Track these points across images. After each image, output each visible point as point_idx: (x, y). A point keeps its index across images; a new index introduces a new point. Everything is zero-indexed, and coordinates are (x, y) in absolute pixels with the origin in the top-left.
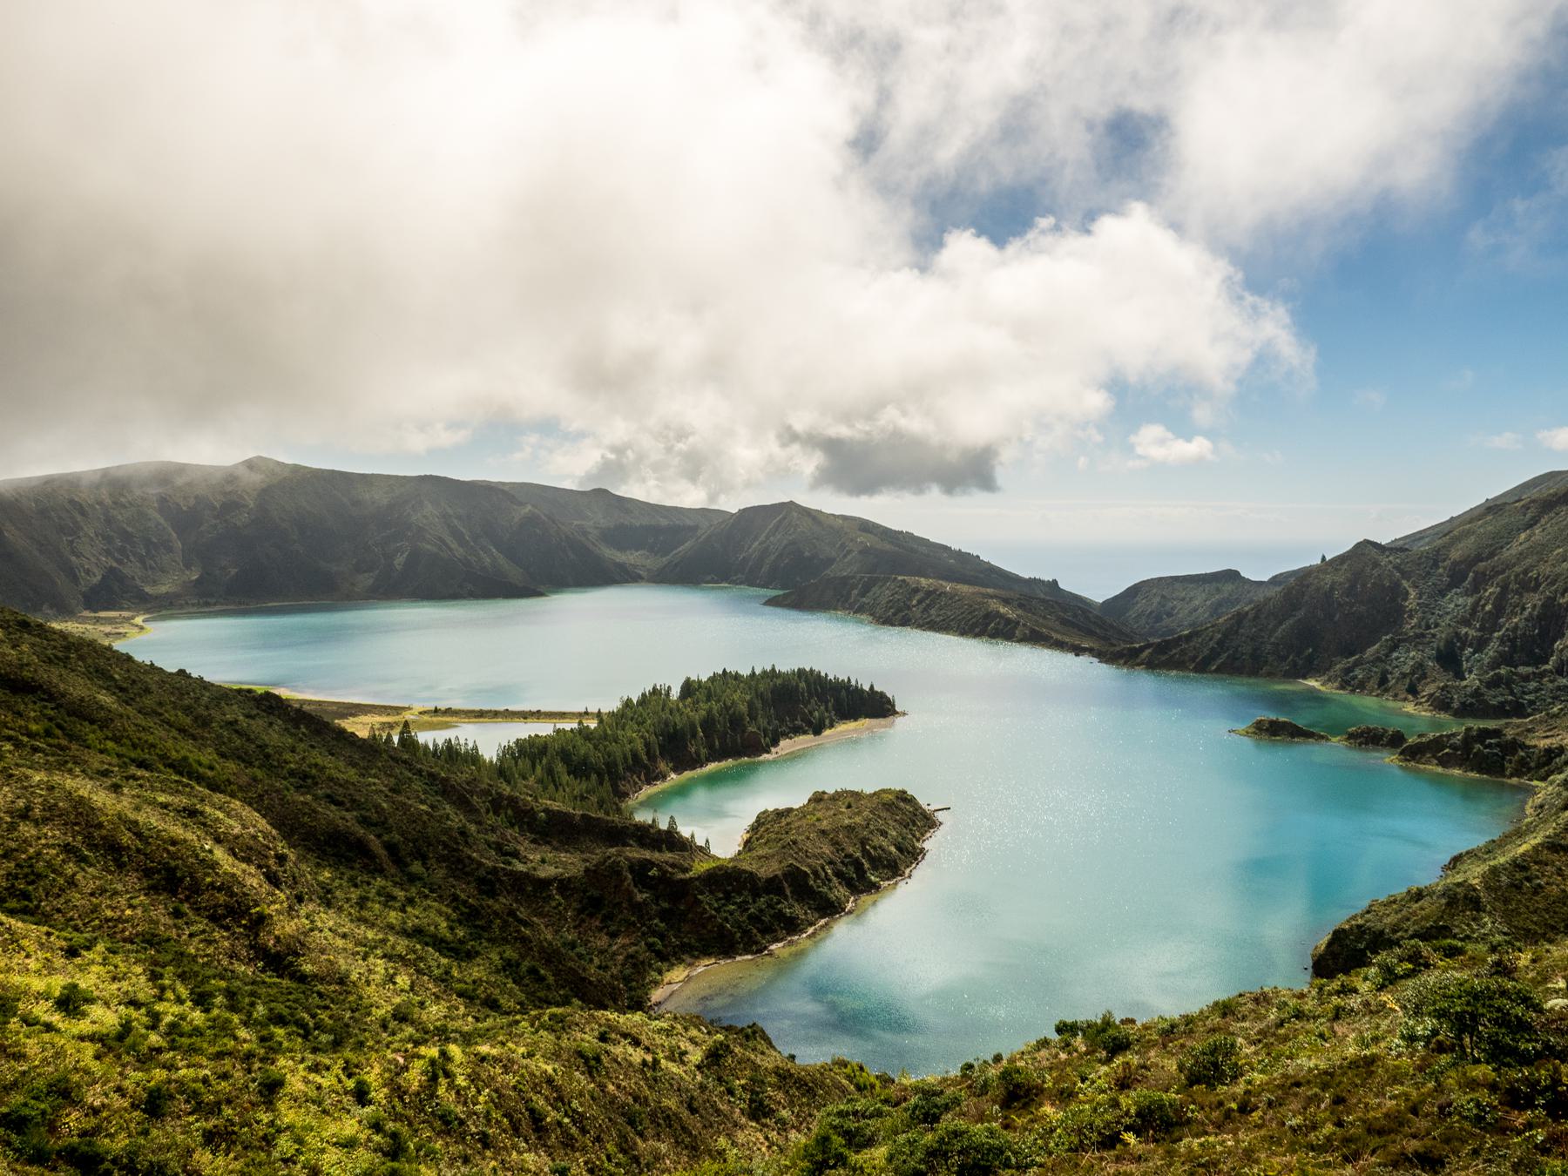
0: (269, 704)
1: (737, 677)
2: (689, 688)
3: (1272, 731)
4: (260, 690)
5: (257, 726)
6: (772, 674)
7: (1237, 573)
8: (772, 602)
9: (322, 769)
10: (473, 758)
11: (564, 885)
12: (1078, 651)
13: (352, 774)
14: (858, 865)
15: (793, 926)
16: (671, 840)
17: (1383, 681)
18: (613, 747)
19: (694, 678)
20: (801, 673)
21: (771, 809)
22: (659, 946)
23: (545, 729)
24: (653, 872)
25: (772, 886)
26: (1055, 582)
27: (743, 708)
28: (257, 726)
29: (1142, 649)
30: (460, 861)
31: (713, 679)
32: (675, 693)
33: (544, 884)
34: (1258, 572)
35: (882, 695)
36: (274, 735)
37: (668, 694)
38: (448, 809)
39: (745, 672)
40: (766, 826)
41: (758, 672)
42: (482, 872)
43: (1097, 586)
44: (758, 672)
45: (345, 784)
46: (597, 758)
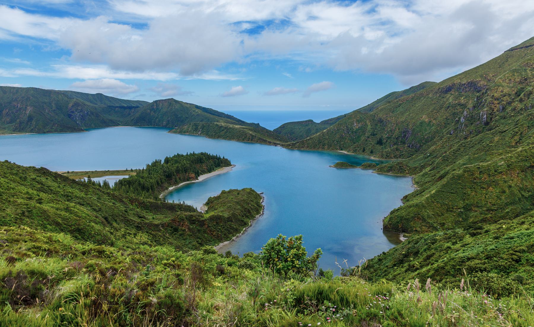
0: (43, 171)
1: (182, 156)
2: (167, 160)
4: (38, 167)
5: (43, 179)
6: (194, 154)
7: (312, 121)
9: (73, 193)
11: (163, 225)
12: (276, 145)
13: (83, 194)
14: (249, 212)
15: (237, 231)
16: (190, 209)
17: (364, 151)
18: (151, 181)
20: (202, 154)
21: (212, 197)
22: (200, 241)
24: (194, 218)
25: (229, 219)
26: (258, 124)
27: (188, 165)
28: (43, 179)
29: (295, 143)
30: (128, 221)
31: (175, 156)
32: (162, 162)
33: (157, 226)
35: (227, 160)
36: (50, 182)
38: (118, 204)
39: (185, 154)
40: (210, 203)
41: (189, 154)
42: (136, 224)
43: (272, 126)
44: (189, 154)
45: (82, 198)
46: (147, 184)
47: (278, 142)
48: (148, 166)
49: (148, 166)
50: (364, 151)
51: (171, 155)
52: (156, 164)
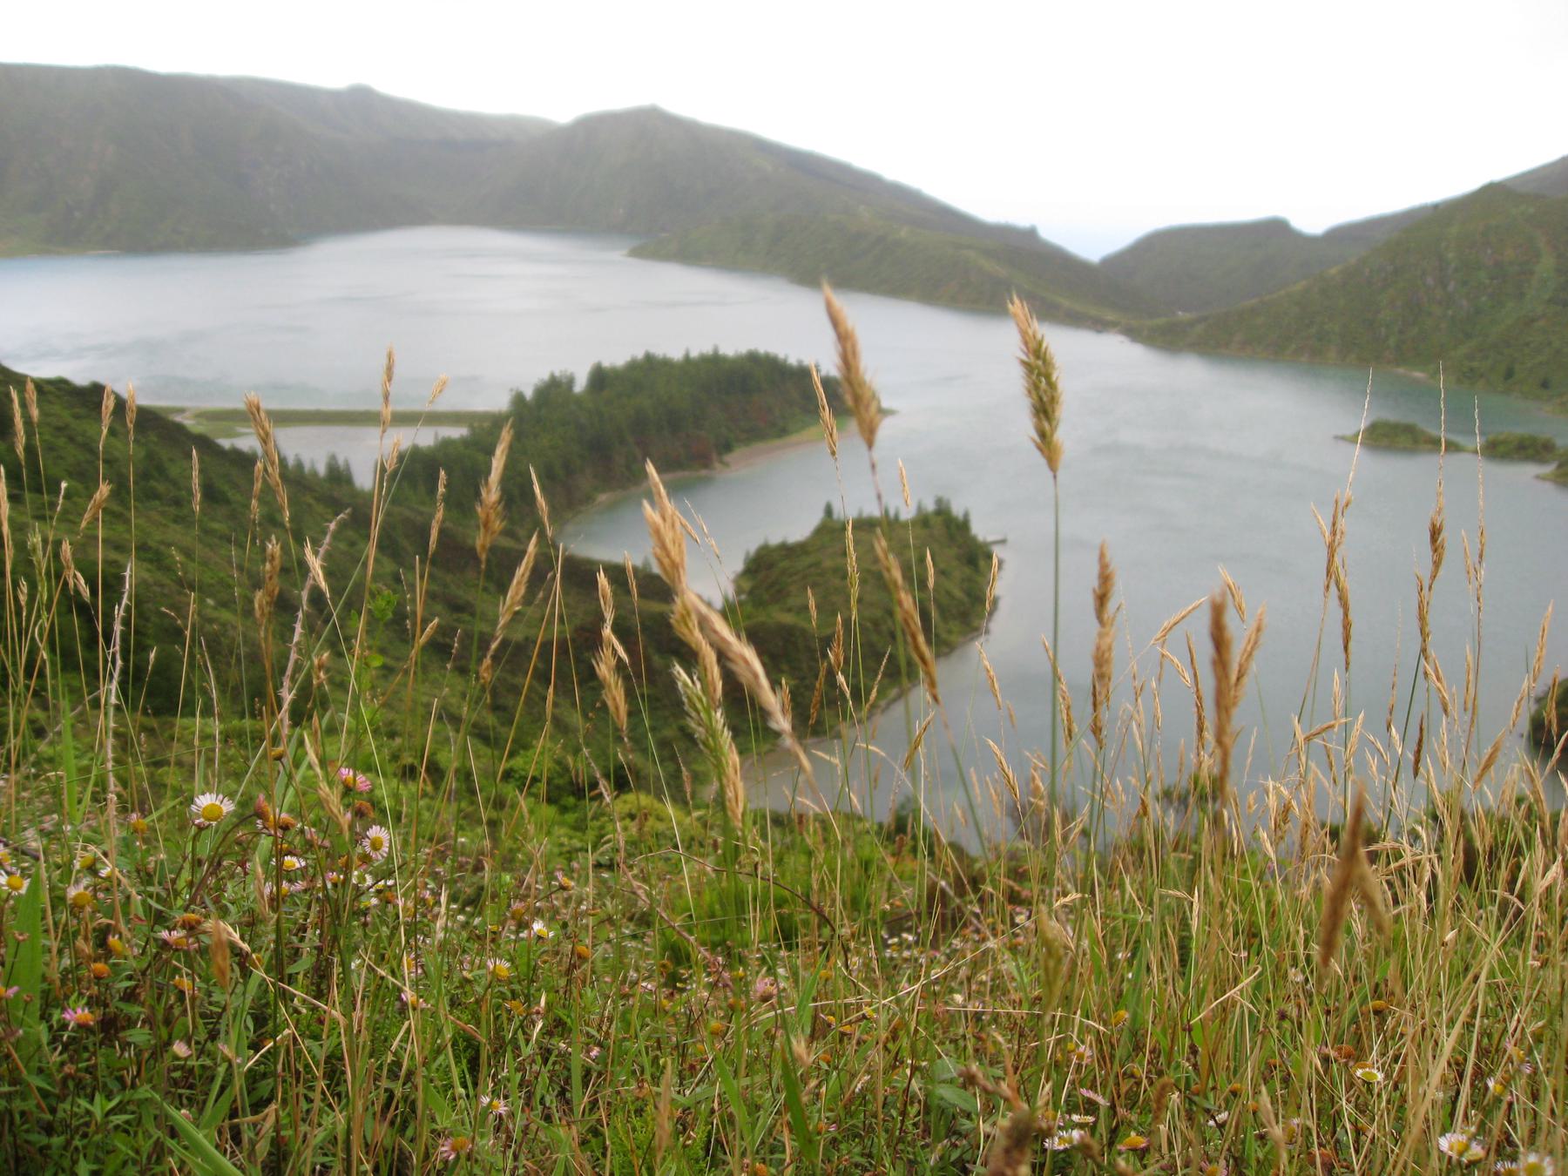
1: (666, 363)
2: (600, 378)
3: (1386, 437)
8: (637, 253)
10: (339, 476)
12: (1100, 325)
17: (1509, 374)
19: (606, 364)
20: (753, 358)
21: (775, 540)
23: (425, 438)
31: (633, 366)
32: (580, 385)
34: (1313, 217)
37: (571, 381)
39: (676, 354)
41: (694, 354)
47: (1110, 316)
48: (519, 399)
49: (519, 399)
50: (1509, 374)
51: (617, 357)
52: (554, 389)
